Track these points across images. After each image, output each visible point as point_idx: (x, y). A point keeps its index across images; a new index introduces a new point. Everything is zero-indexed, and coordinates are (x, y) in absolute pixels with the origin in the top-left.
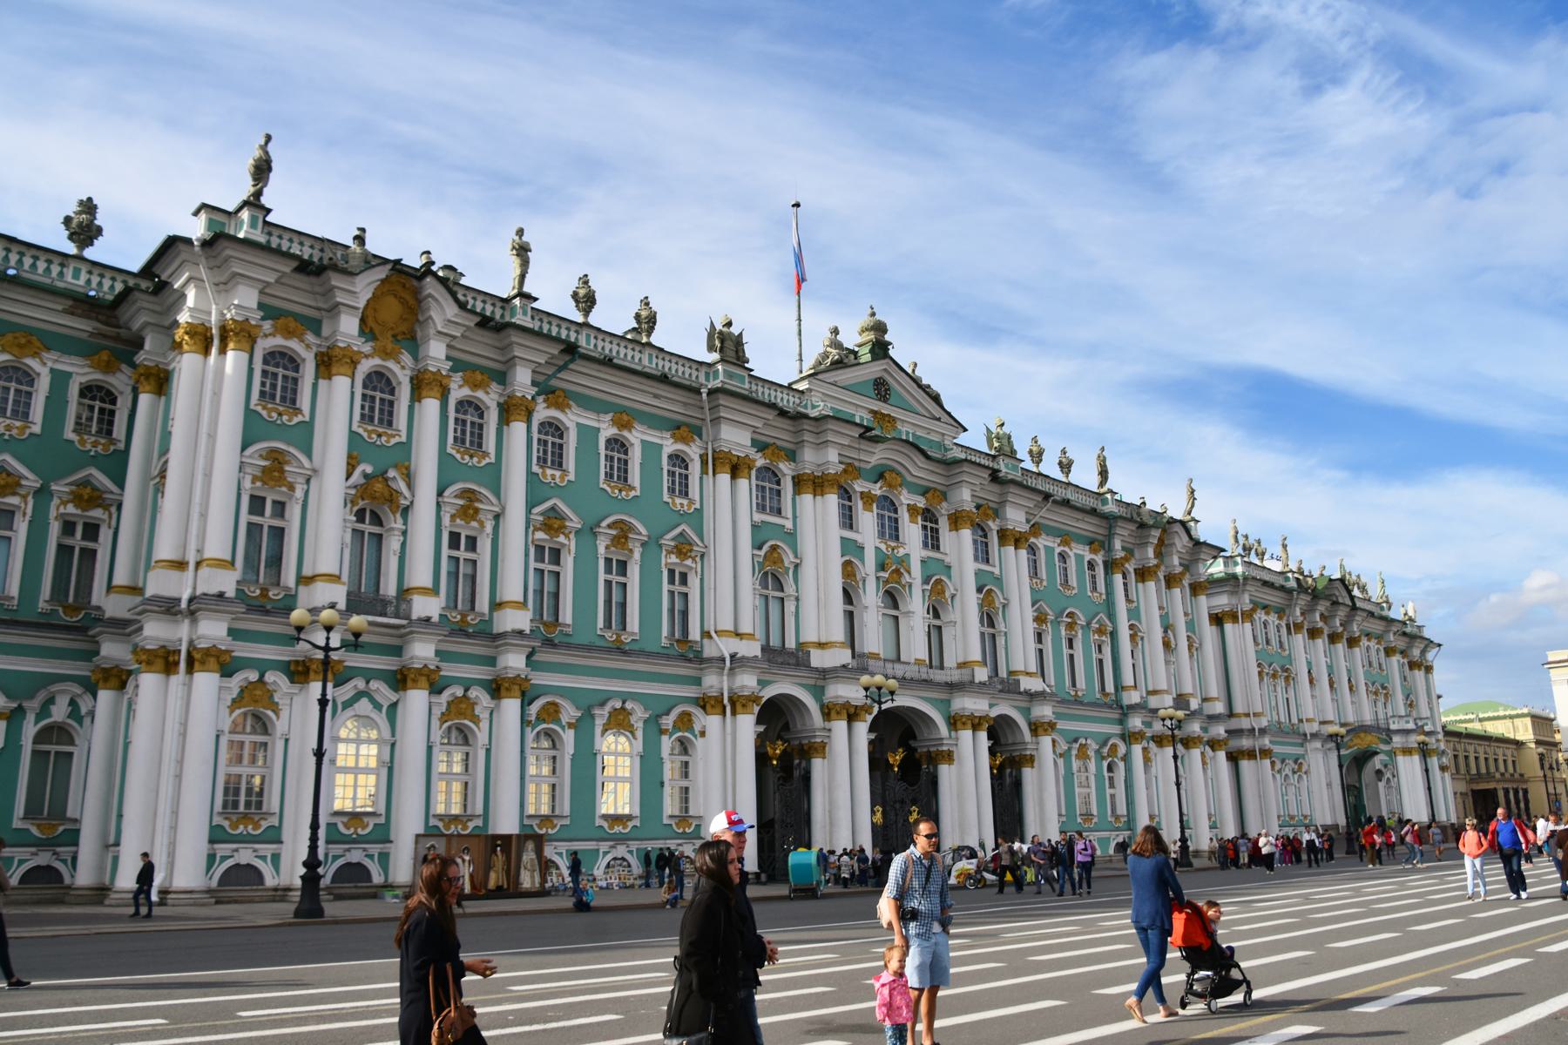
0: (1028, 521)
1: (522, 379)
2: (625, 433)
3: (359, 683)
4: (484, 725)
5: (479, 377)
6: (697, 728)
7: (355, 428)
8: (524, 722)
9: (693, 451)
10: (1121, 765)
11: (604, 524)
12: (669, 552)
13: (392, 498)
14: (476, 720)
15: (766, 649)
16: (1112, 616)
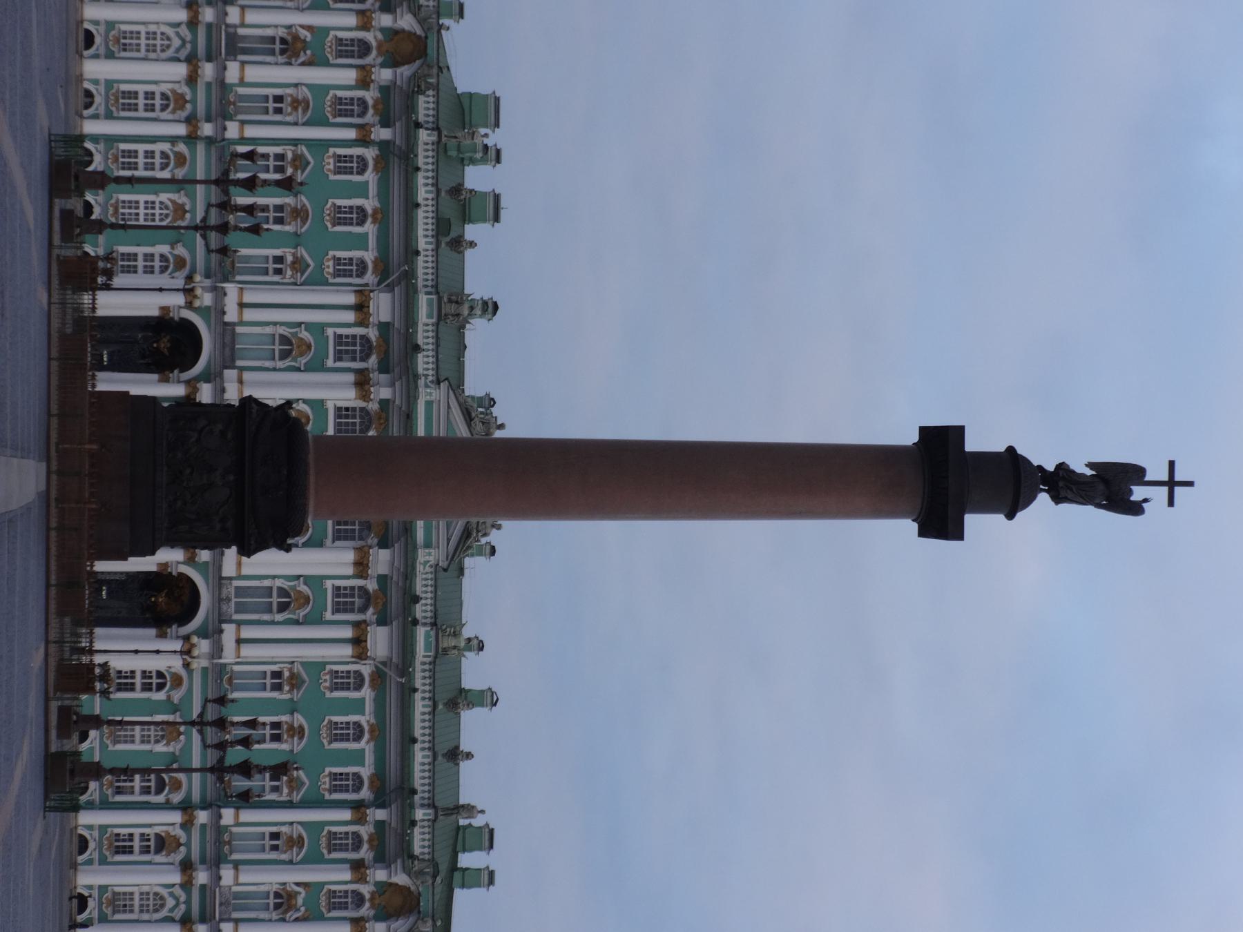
0: (384, 663)
1: (384, 134)
2: (370, 220)
3: (189, 37)
4: (170, 117)
5: (380, 107)
6: (177, 274)
7: (332, 33)
8: (173, 140)
9: (370, 278)
10: (161, 798)
11: (303, 198)
12: (294, 255)
13: (297, 55)
14: (173, 112)
15: (233, 324)
16: (305, 804)
